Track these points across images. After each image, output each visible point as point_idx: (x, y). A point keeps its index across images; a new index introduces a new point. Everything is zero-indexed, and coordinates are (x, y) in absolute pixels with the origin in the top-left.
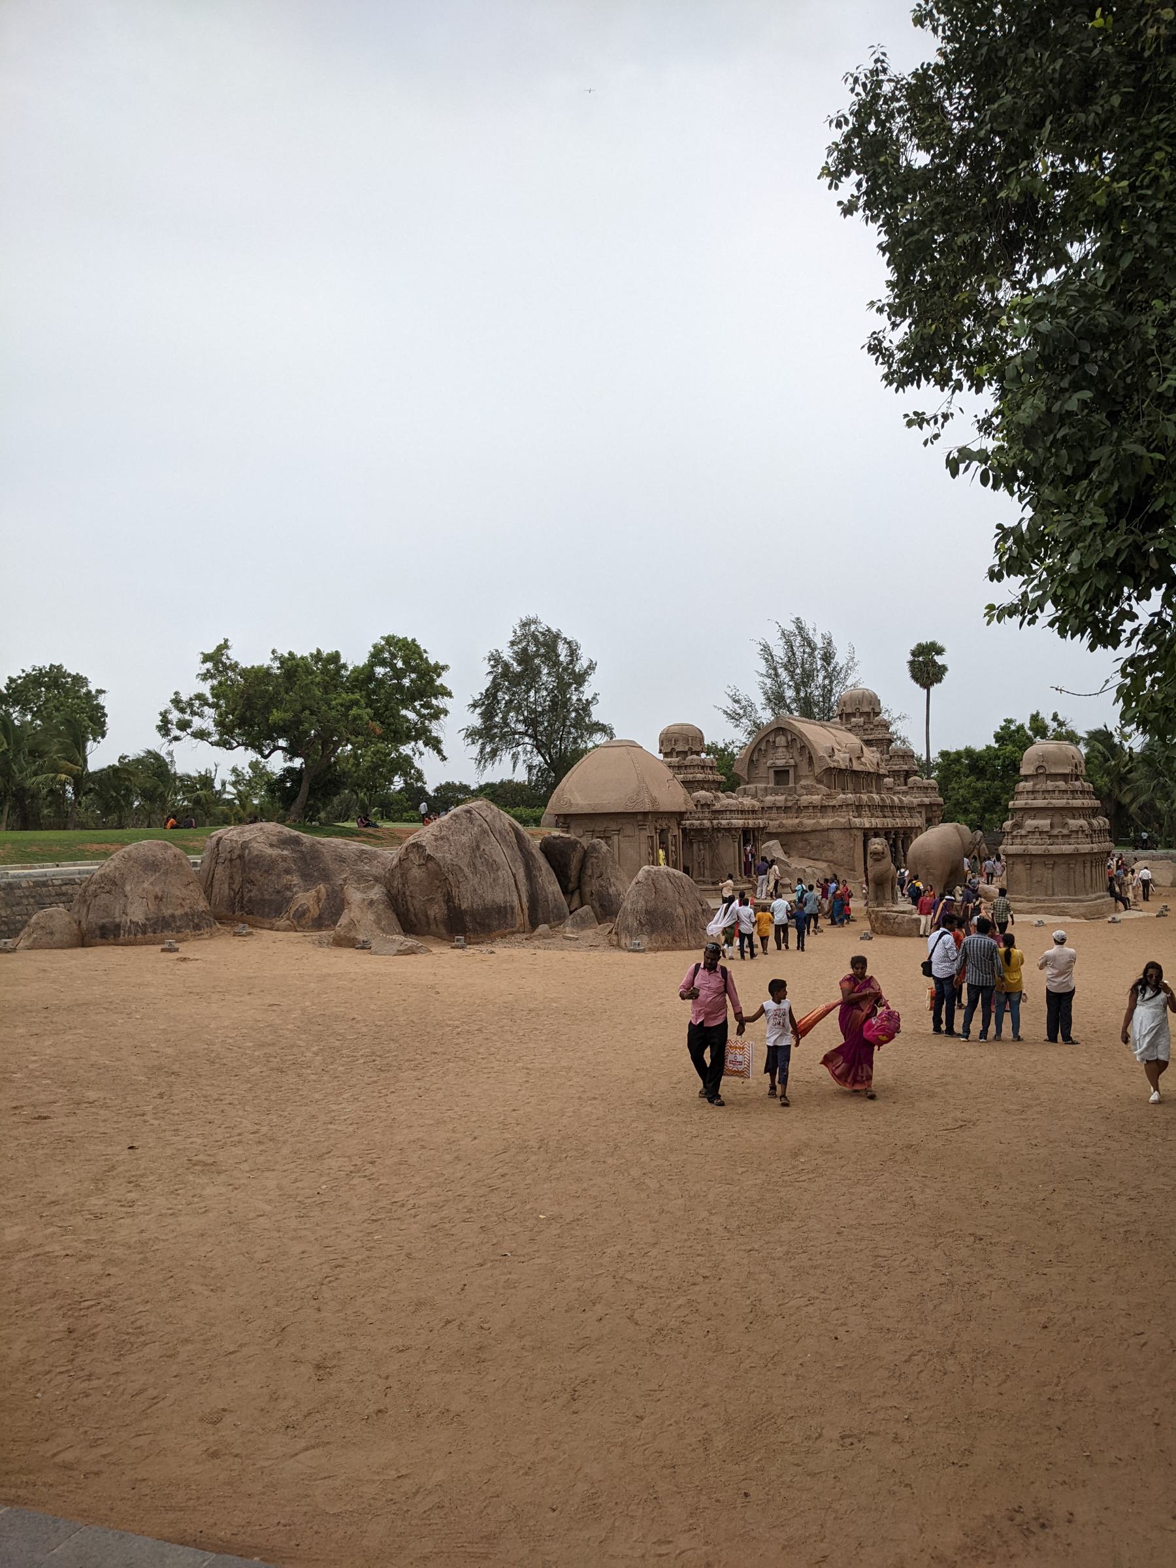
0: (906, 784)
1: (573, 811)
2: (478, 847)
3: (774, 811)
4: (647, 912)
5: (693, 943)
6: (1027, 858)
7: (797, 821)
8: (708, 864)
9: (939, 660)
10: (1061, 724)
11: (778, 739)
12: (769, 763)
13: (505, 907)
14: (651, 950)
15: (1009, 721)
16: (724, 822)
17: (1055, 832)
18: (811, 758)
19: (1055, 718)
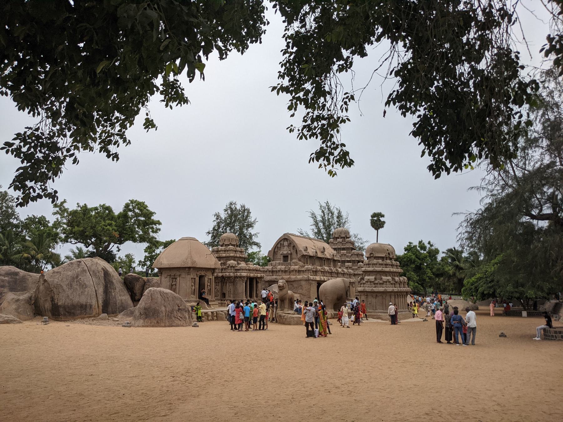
1: (162, 266)
2: (77, 277)
4: (145, 309)
5: (167, 324)
7: (288, 276)
8: (232, 292)
9: (382, 219)
10: (432, 246)
13: (86, 305)
14: (143, 326)
15: (410, 243)
16: (239, 274)
17: (376, 282)
19: (429, 243)
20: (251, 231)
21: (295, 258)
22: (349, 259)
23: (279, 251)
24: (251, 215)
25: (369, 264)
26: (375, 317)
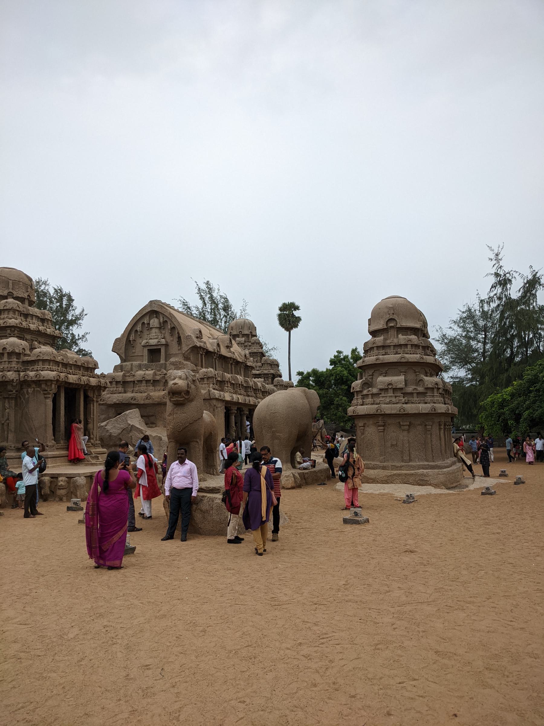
0: (272, 383)
3: (144, 384)
6: (380, 419)
8: (12, 426)
11: (152, 321)
12: (144, 342)
15: (339, 352)
16: (32, 374)
17: (410, 389)
18: (179, 338)
20: (76, 330)
21: (175, 355)
22: (258, 372)
23: (139, 340)
24: (74, 304)
25: (383, 347)
26: (411, 479)
